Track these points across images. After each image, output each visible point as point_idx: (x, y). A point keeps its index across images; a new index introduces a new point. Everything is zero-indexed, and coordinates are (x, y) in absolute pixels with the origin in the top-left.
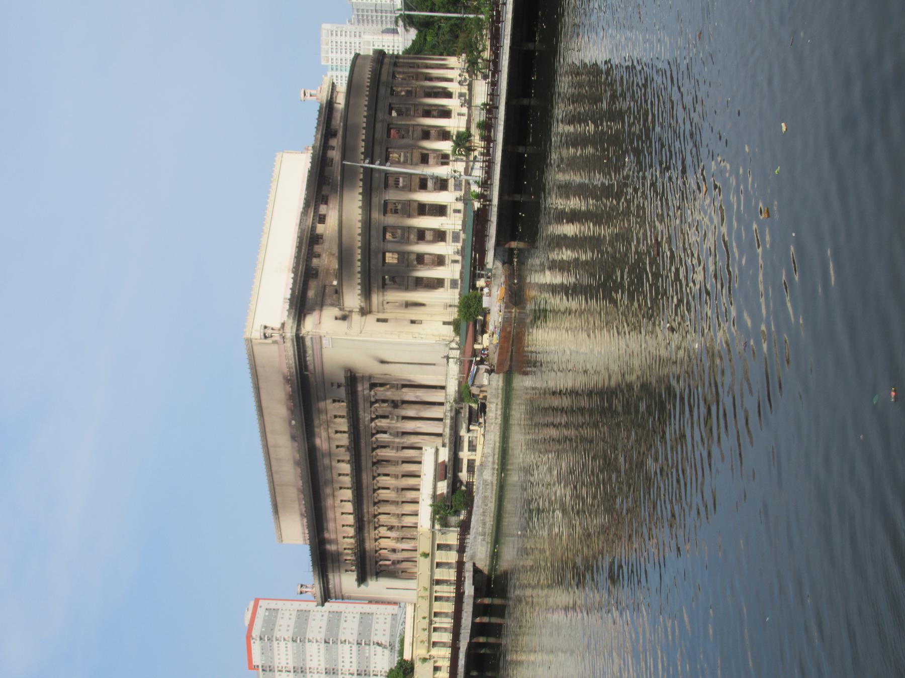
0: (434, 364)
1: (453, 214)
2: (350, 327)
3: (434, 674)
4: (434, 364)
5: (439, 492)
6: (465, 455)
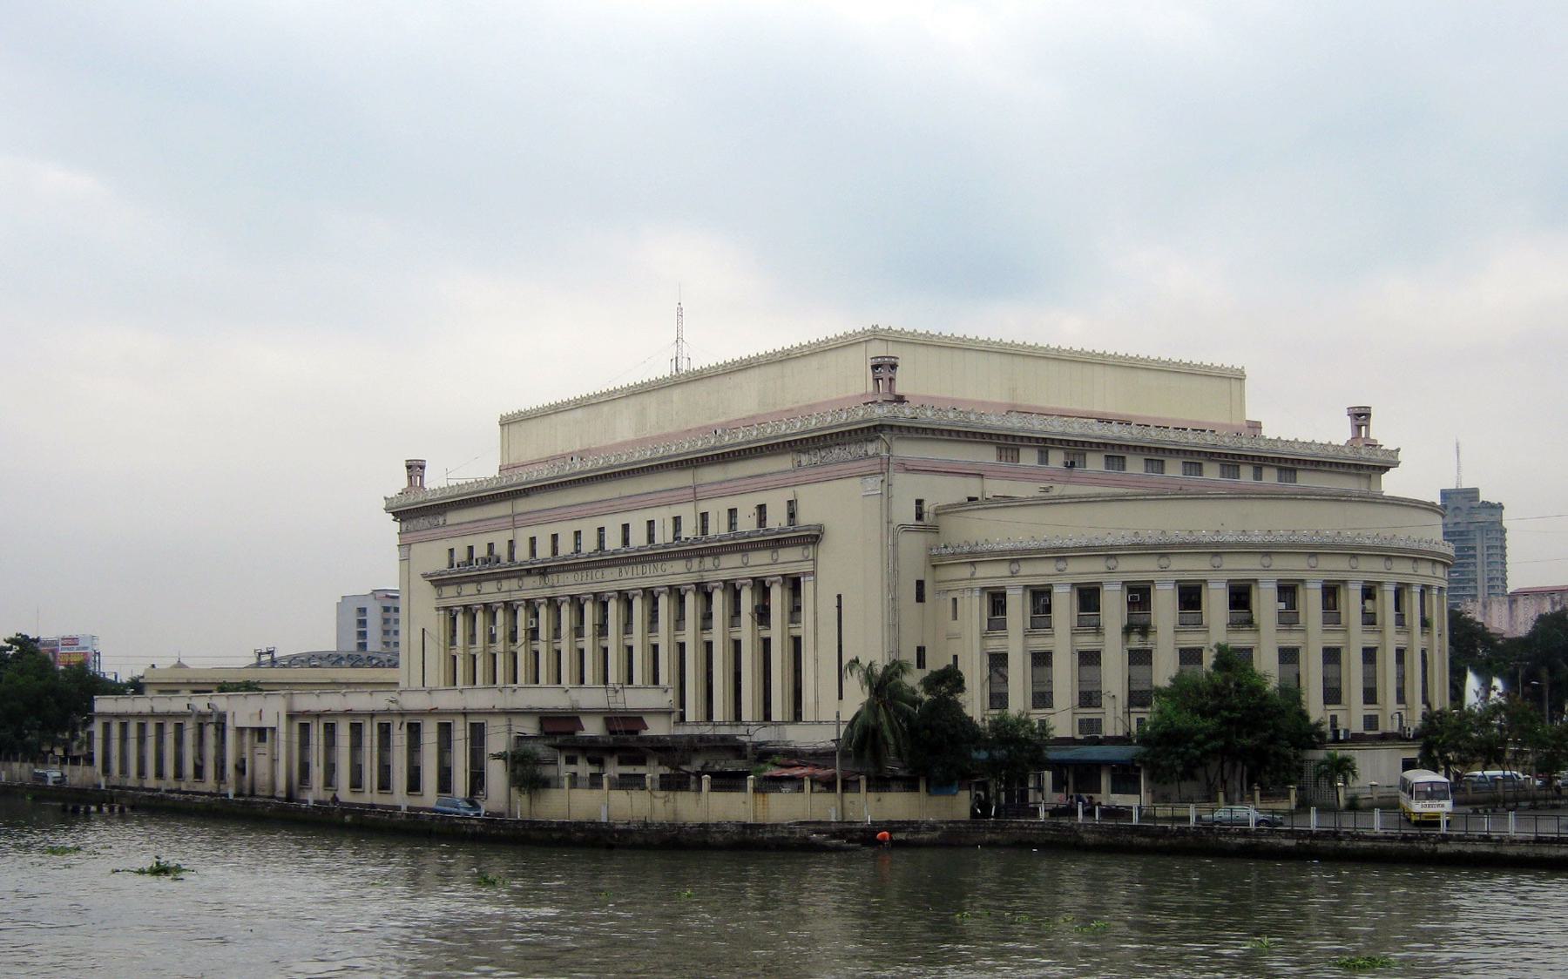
0: (841, 697)
1: (1134, 718)
2: (906, 528)
3: (253, 729)
4: (841, 697)
5: (585, 721)
6: (652, 771)
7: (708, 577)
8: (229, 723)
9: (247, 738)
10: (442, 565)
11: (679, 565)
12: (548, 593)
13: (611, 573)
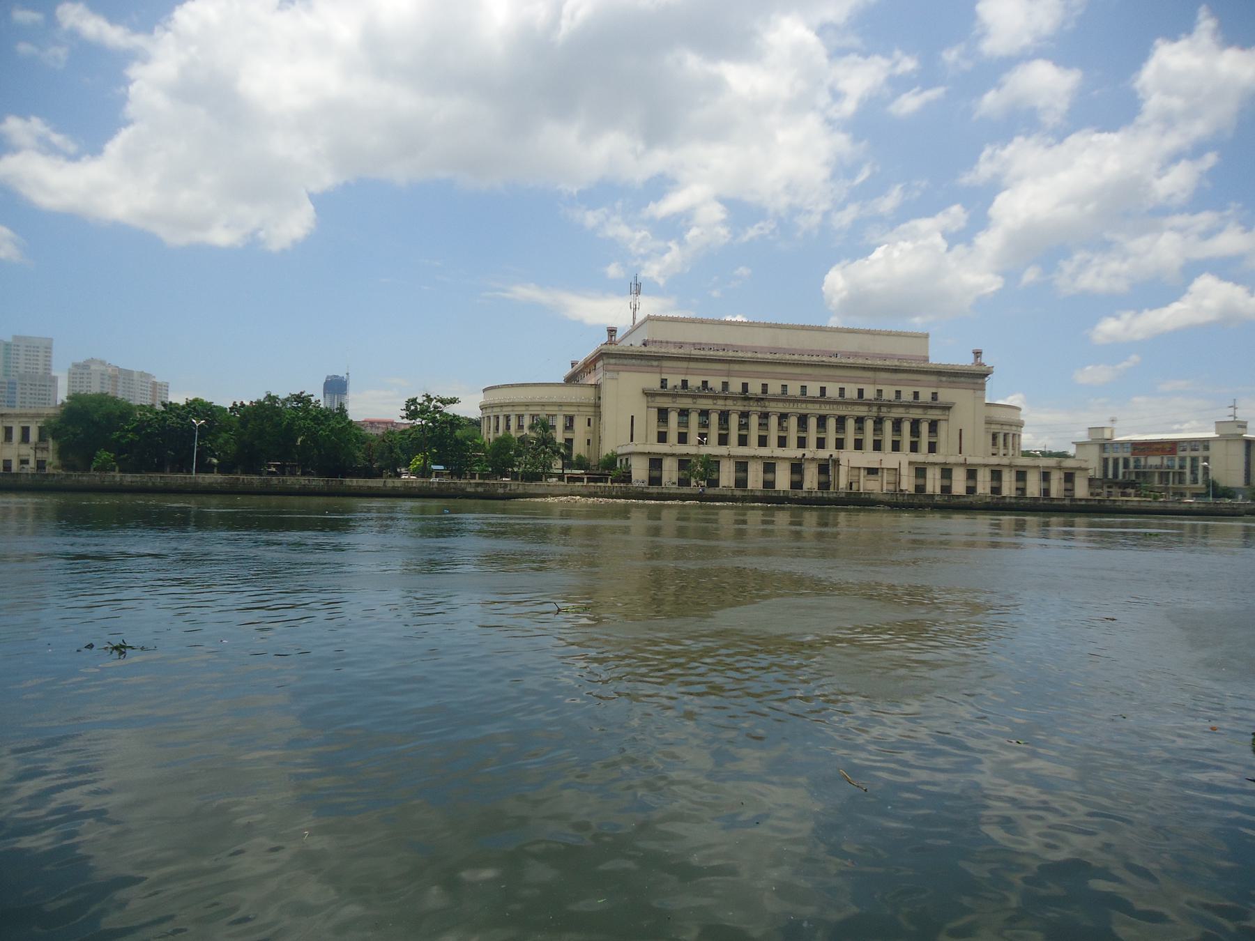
7: (882, 415)
8: (843, 462)
9: (863, 473)
10: (655, 384)
11: (865, 408)
12: (759, 409)
13: (810, 406)
